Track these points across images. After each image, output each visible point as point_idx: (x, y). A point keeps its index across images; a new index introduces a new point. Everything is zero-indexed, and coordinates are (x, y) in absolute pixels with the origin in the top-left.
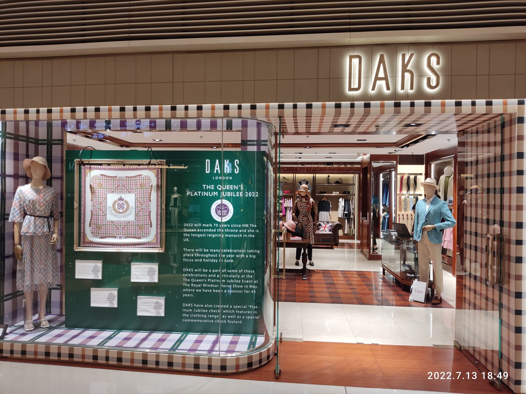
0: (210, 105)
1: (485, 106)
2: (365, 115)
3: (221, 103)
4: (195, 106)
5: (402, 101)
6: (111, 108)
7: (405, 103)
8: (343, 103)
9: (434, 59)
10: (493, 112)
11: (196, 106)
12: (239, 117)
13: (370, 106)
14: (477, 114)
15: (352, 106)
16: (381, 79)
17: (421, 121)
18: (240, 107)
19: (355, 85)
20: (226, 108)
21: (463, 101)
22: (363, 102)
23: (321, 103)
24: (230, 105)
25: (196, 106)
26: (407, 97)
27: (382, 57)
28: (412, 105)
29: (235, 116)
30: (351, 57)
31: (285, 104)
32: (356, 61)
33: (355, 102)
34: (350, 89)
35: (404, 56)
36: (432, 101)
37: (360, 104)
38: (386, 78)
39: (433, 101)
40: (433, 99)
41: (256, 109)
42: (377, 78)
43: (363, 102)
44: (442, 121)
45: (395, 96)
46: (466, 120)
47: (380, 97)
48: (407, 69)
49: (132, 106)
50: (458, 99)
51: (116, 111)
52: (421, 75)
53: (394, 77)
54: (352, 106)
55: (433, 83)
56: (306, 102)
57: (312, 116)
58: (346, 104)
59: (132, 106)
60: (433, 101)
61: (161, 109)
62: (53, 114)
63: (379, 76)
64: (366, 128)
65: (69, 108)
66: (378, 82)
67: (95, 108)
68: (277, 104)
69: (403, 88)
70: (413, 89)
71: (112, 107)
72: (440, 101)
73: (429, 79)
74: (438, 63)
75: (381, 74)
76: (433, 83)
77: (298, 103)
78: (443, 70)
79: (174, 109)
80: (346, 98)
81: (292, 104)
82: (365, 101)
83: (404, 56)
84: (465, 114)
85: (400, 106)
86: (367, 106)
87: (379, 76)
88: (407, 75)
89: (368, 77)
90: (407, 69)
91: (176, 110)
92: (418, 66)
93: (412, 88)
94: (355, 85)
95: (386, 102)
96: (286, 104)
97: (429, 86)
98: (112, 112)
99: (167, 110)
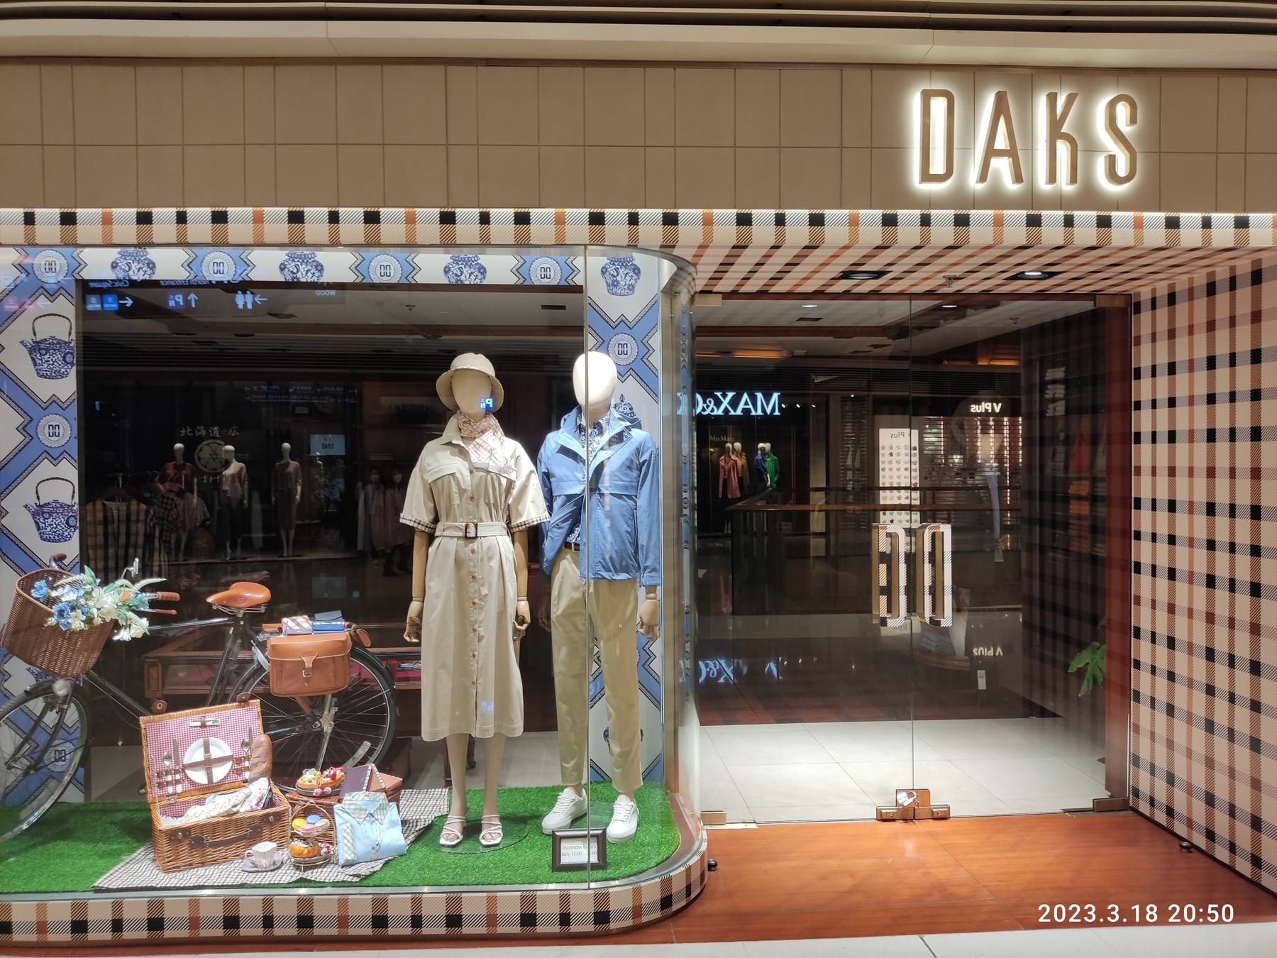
0: (551, 211)
1: (1164, 230)
2: (630, 243)
3: (585, 207)
4: (805, 213)
5: (1044, 213)
6: (261, 214)
7: (1052, 216)
8: (901, 213)
9: (1122, 111)
10: (1112, 244)
11: (585, 212)
12: (629, 246)
13: (824, 221)
14: (933, 248)
15: (925, 221)
16: (1001, 153)
17: (871, 265)
18: (633, 220)
19: (938, 167)
20: (597, 220)
21: (1184, 216)
22: (952, 212)
23: (701, 210)
24: (607, 211)
25: (511, 212)
26: (1058, 202)
27: (1000, 98)
28: (1069, 222)
29: (205, 241)
30: (927, 96)
31: (607, 211)
32: (939, 105)
33: (933, 212)
34: (927, 177)
35: (1052, 99)
36: (972, 212)
37: (944, 216)
38: (1011, 153)
39: (1115, 214)
40: (1118, 209)
41: (824, 225)
42: (990, 152)
43: (952, 212)
44: (927, 264)
45: (1031, 200)
46: (936, 264)
47: (996, 200)
48: (1062, 131)
49: (326, 210)
50: (1171, 211)
51: (92, 223)
52: (1092, 148)
53: (1031, 149)
54: (925, 221)
55: (1122, 170)
56: (810, 209)
57: (678, 244)
58: (908, 216)
59: (326, 210)
60: (1115, 214)
61: (258, 219)
62: (1113, 230)
63: (996, 147)
64: (737, 282)
65: (132, 212)
66: (996, 163)
67: (212, 212)
68: (587, 211)
69: (1052, 178)
70: (1022, 181)
71: (266, 209)
72: (1131, 214)
73: (1112, 160)
74: (1133, 120)
75: (1001, 143)
76: (1122, 170)
77: (189, 210)
78: (1143, 136)
79: (448, 219)
80: (911, 201)
81: (773, 212)
82: (956, 209)
83: (1052, 99)
84: (938, 247)
85: (1040, 225)
86: (962, 221)
87: (996, 147)
88: (1063, 148)
89: (968, 148)
90: (1062, 131)
91: (750, 224)
92: (1084, 124)
93: (1073, 179)
94: (938, 167)
95: (1006, 212)
96: (608, 212)
97: (1113, 176)
98: (265, 225)
99: (428, 221)
